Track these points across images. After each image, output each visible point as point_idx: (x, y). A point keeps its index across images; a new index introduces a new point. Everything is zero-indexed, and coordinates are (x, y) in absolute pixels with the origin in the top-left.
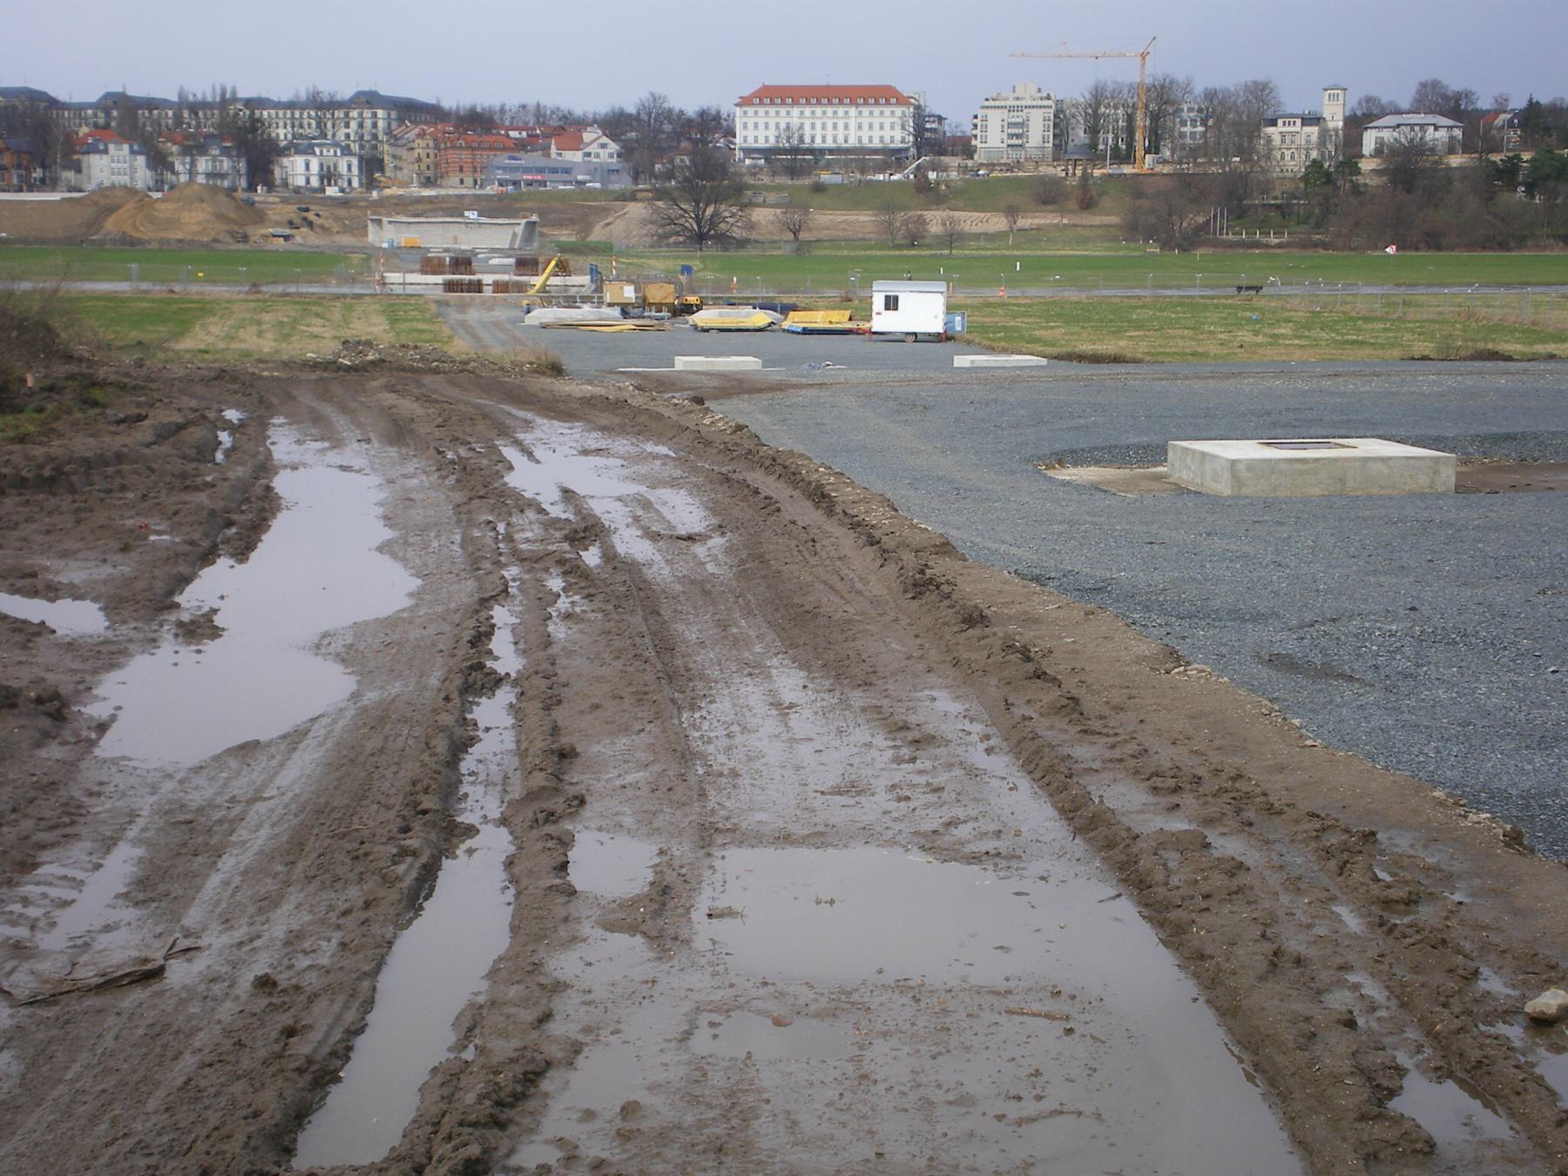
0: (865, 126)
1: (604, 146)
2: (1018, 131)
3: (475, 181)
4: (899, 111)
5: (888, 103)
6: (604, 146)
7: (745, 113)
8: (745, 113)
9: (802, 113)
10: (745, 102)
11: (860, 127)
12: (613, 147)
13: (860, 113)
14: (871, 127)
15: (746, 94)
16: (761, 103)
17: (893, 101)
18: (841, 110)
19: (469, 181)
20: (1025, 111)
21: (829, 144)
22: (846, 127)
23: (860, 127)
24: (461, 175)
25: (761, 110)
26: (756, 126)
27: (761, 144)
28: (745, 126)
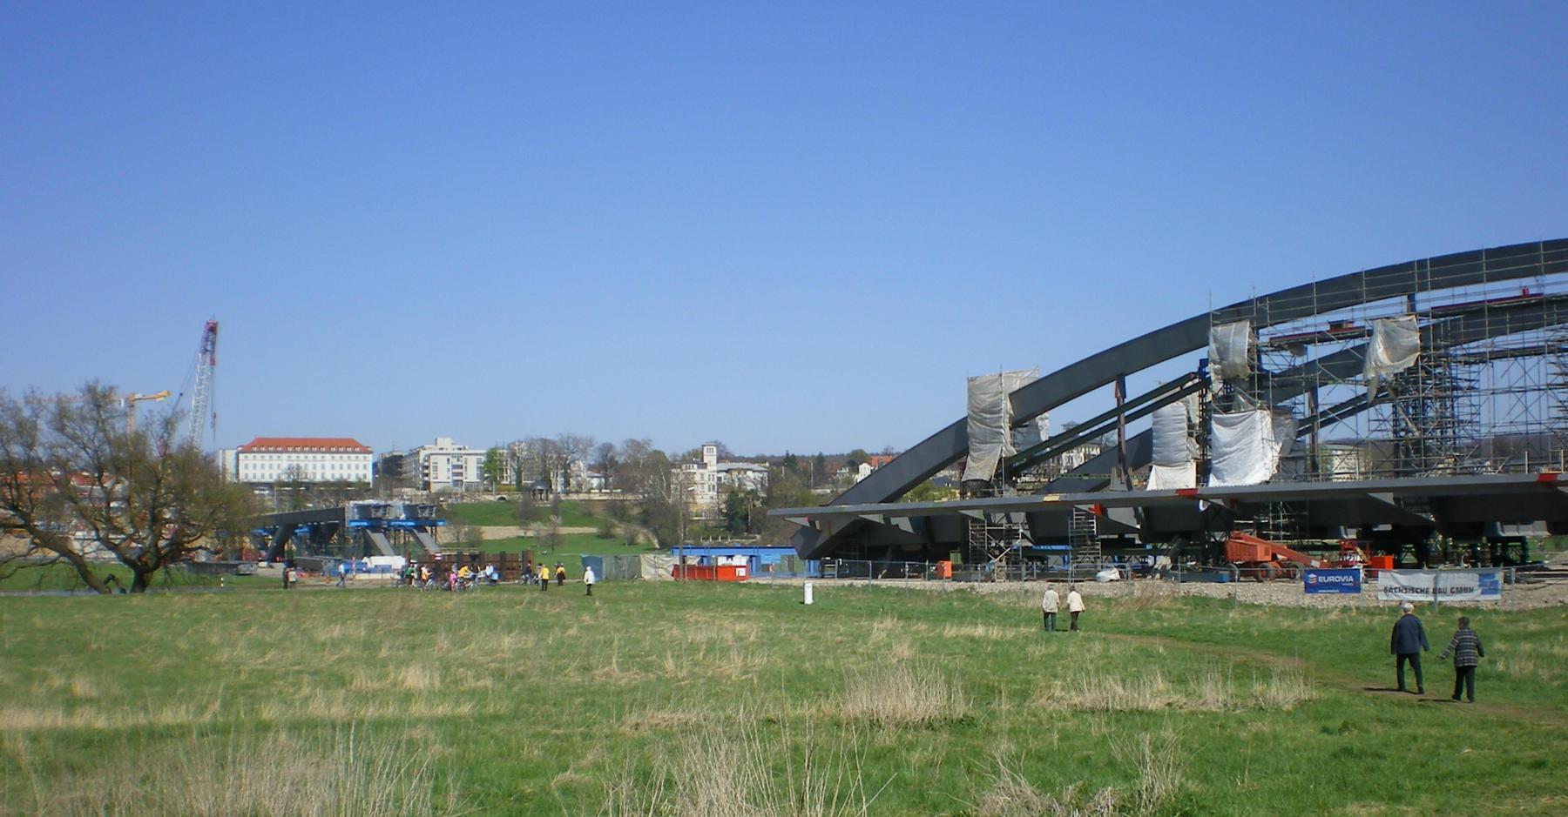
0: (337, 467)
2: (458, 469)
4: (361, 456)
8: (246, 457)
9: (289, 457)
10: (247, 450)
11: (333, 467)
13: (333, 457)
14: (349, 467)
15: (245, 444)
17: (358, 450)
18: (319, 456)
20: (464, 457)
21: (318, 479)
22: (323, 467)
23: (333, 467)
27: (267, 479)
28: (246, 466)
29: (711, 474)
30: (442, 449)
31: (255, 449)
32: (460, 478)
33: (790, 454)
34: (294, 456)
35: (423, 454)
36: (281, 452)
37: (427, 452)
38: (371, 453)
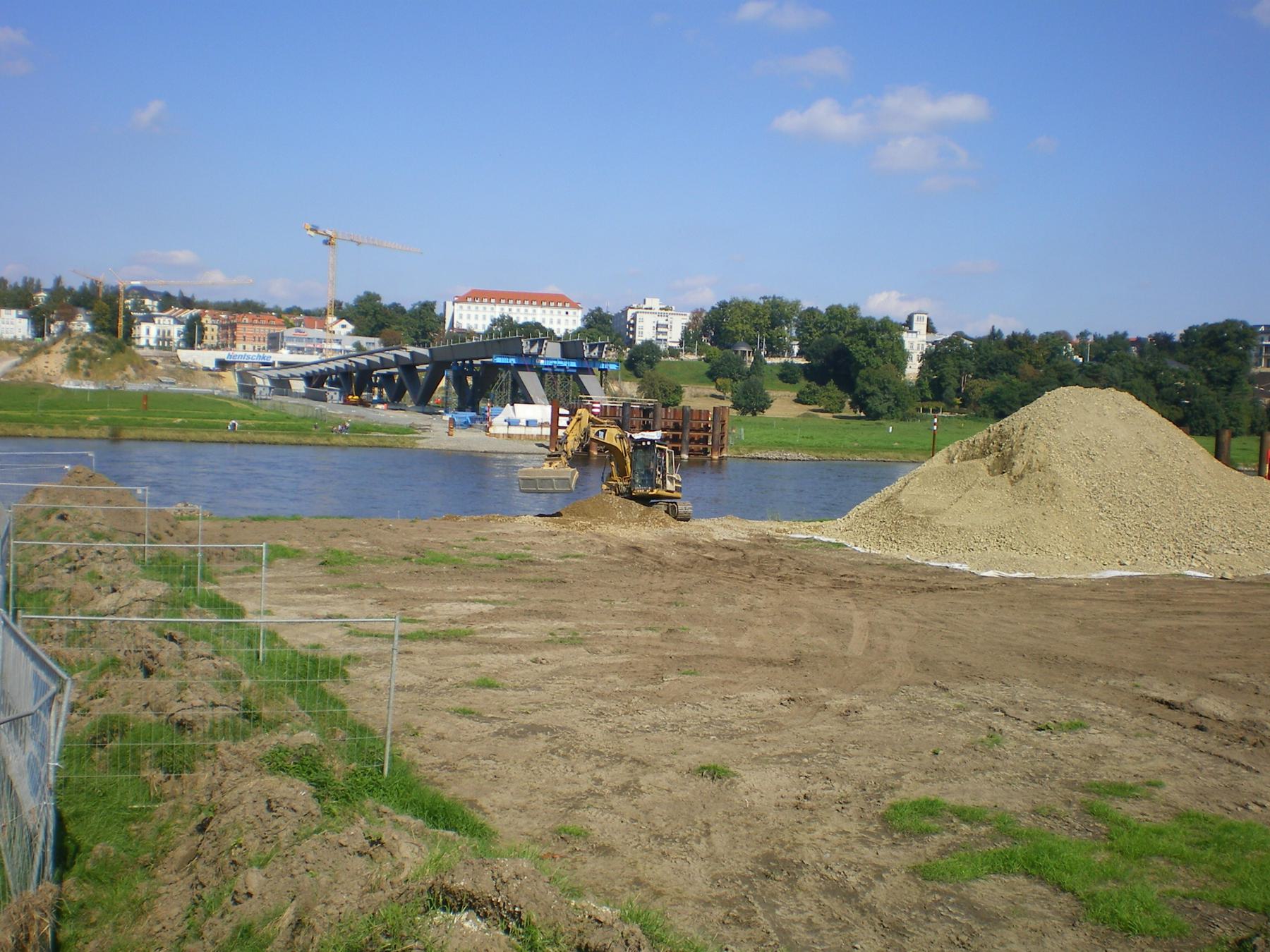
1: (344, 326)
3: (254, 347)
4: (571, 312)
5: (564, 306)
6: (344, 326)
7: (461, 307)
10: (463, 299)
12: (350, 327)
13: (544, 311)
15: (461, 295)
16: (474, 301)
17: (567, 305)
18: (530, 309)
19: (249, 347)
24: (244, 343)
25: (473, 306)
26: (469, 317)
28: (461, 316)
29: (921, 343)
30: (651, 309)
31: (469, 300)
32: (664, 337)
33: (996, 330)
34: (506, 308)
35: (630, 312)
36: (495, 304)
37: (634, 311)
38: (579, 308)
